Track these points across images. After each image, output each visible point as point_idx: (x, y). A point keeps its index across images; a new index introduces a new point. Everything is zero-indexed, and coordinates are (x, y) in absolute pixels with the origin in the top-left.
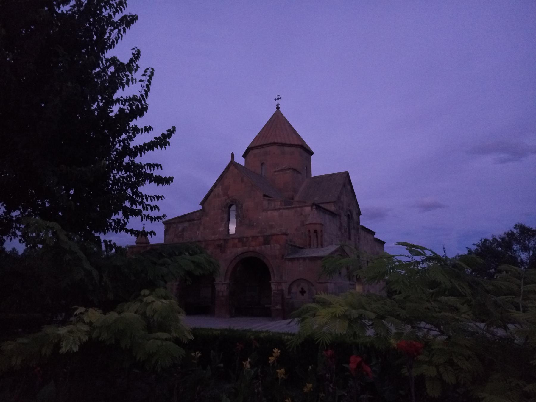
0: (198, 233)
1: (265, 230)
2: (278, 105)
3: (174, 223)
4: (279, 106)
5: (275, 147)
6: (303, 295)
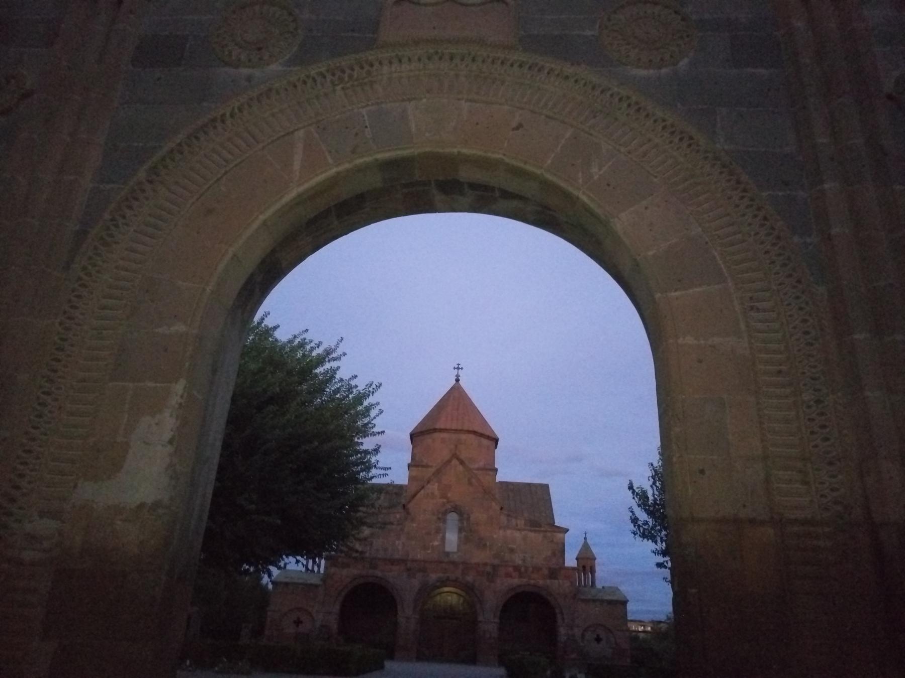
2: (458, 376)
4: (459, 378)
5: (472, 436)
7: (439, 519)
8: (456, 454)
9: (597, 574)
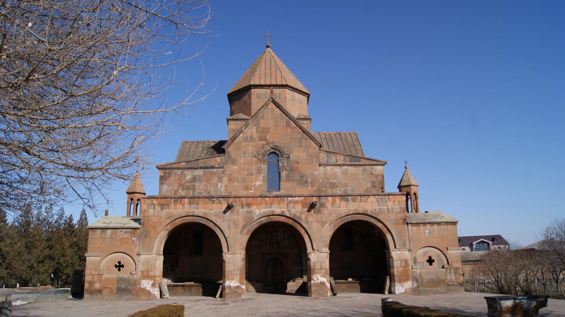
0: (219, 186)
1: (324, 189)
3: (179, 169)
5: (287, 90)
6: (431, 264)
7: (261, 160)
8: (272, 98)
9: (420, 201)
